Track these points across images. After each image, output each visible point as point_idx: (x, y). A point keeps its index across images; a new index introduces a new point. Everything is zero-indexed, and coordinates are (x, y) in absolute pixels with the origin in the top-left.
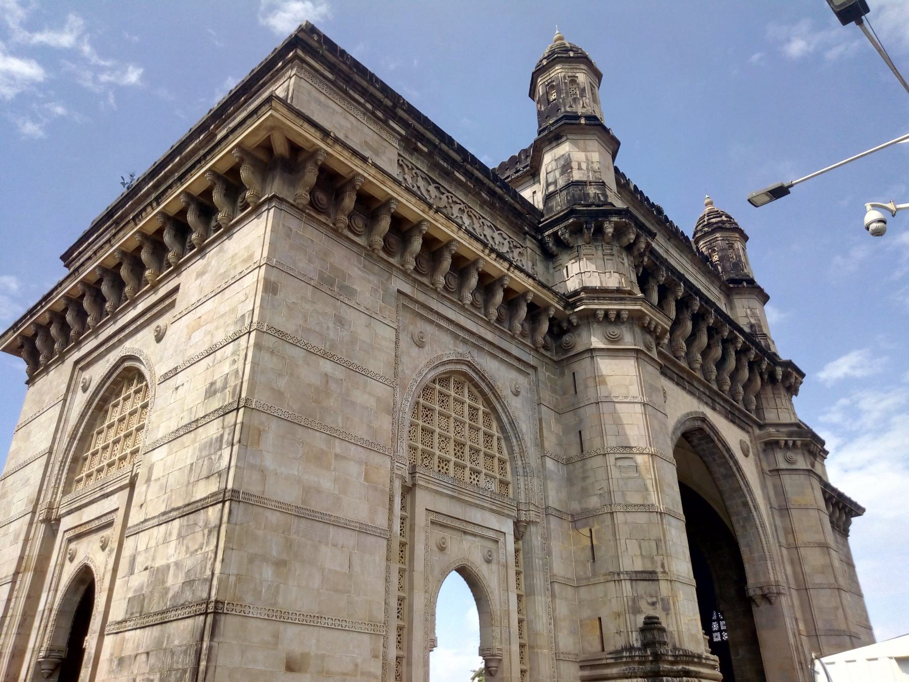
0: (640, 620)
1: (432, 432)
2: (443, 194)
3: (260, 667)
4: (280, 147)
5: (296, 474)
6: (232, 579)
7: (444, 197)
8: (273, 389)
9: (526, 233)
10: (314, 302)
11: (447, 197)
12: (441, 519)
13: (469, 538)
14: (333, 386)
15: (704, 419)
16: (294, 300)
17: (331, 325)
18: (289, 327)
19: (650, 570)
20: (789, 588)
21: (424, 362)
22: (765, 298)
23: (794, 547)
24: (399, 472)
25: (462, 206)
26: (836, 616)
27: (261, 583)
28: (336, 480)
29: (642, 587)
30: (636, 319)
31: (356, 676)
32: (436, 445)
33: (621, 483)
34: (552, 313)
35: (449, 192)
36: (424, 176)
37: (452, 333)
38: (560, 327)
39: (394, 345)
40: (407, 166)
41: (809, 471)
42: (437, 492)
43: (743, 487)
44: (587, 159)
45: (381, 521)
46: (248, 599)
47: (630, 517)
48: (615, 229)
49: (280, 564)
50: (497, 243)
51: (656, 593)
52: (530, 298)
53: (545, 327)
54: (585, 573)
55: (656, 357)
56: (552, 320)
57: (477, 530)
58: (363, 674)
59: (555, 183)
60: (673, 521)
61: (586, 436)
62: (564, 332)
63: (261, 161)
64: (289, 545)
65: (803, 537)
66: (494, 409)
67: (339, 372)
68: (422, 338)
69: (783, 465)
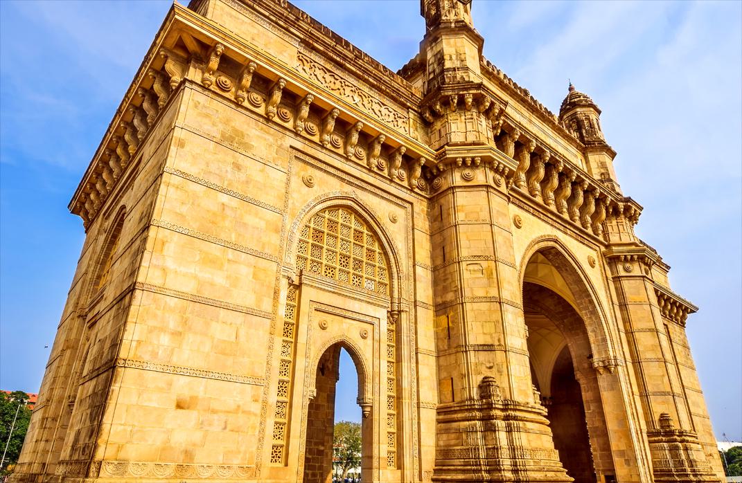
0: (480, 378)
1: (322, 248)
2: (337, 80)
3: (154, 404)
4: (192, 46)
5: (193, 272)
6: (134, 344)
7: (337, 82)
8: (176, 213)
9: (409, 108)
10: (215, 153)
11: (341, 82)
12: (323, 307)
13: (348, 320)
14: (228, 212)
15: (556, 241)
16: (198, 152)
17: (229, 169)
18: (193, 171)
19: (490, 343)
20: (626, 361)
21: (313, 198)
22: (613, 155)
23: (630, 333)
24: (286, 274)
25: (354, 89)
26: (663, 382)
27: (158, 347)
28: (228, 277)
29: (483, 356)
30: (488, 162)
31: (237, 413)
32: (324, 257)
33: (470, 282)
34: (423, 161)
35: (342, 78)
36: (321, 67)
37: (338, 177)
38: (432, 173)
39: (284, 185)
40: (307, 61)
41: (643, 277)
42: (321, 289)
43: (589, 289)
44: (457, 52)
45: (267, 306)
46: (146, 357)
47: (476, 306)
48: (474, 100)
49: (177, 334)
50: (383, 115)
51: (493, 359)
52: (403, 150)
53: (418, 172)
54: (443, 347)
55: (505, 191)
56: (424, 168)
57: (355, 316)
58: (244, 412)
59: (434, 71)
60: (510, 308)
61: (447, 249)
62: (434, 177)
63: (182, 57)
64: (185, 322)
65: (636, 325)
66: (375, 233)
67: (234, 203)
68: (310, 180)
69: (622, 273)
